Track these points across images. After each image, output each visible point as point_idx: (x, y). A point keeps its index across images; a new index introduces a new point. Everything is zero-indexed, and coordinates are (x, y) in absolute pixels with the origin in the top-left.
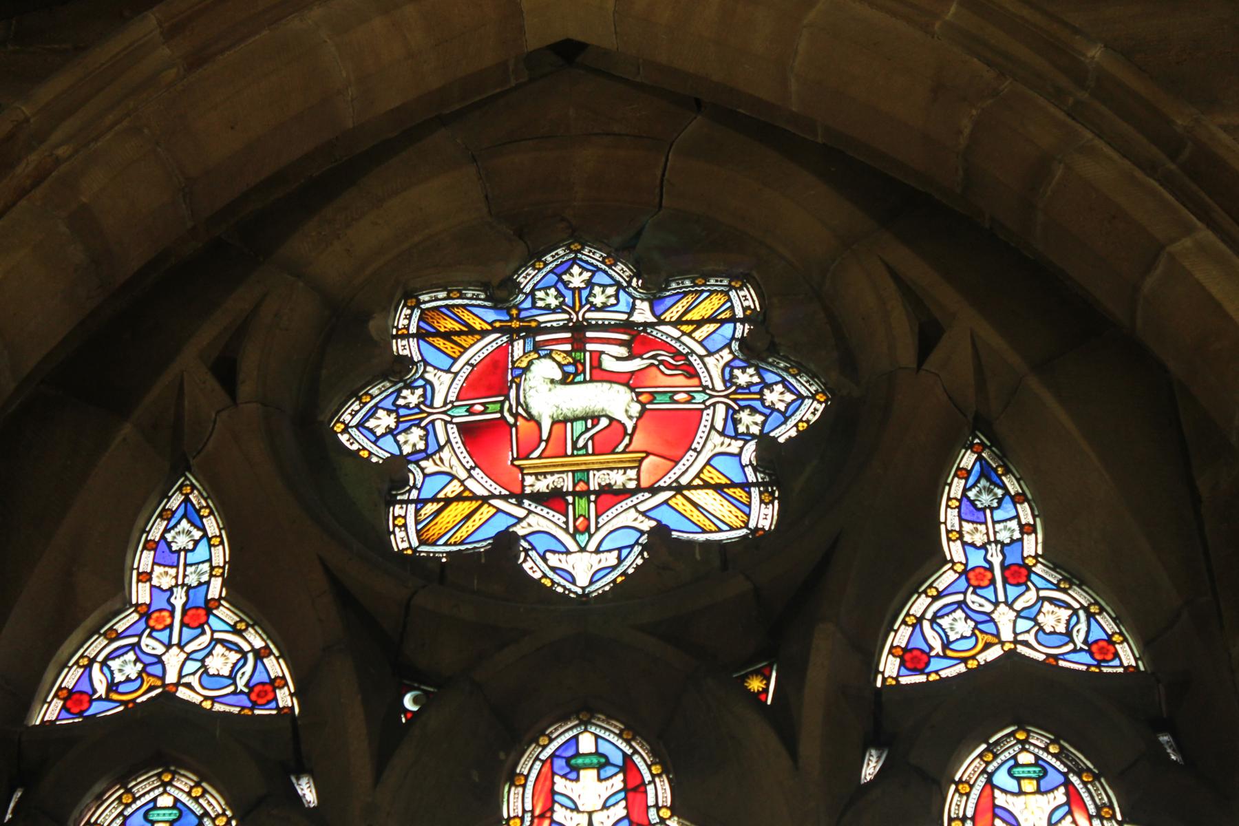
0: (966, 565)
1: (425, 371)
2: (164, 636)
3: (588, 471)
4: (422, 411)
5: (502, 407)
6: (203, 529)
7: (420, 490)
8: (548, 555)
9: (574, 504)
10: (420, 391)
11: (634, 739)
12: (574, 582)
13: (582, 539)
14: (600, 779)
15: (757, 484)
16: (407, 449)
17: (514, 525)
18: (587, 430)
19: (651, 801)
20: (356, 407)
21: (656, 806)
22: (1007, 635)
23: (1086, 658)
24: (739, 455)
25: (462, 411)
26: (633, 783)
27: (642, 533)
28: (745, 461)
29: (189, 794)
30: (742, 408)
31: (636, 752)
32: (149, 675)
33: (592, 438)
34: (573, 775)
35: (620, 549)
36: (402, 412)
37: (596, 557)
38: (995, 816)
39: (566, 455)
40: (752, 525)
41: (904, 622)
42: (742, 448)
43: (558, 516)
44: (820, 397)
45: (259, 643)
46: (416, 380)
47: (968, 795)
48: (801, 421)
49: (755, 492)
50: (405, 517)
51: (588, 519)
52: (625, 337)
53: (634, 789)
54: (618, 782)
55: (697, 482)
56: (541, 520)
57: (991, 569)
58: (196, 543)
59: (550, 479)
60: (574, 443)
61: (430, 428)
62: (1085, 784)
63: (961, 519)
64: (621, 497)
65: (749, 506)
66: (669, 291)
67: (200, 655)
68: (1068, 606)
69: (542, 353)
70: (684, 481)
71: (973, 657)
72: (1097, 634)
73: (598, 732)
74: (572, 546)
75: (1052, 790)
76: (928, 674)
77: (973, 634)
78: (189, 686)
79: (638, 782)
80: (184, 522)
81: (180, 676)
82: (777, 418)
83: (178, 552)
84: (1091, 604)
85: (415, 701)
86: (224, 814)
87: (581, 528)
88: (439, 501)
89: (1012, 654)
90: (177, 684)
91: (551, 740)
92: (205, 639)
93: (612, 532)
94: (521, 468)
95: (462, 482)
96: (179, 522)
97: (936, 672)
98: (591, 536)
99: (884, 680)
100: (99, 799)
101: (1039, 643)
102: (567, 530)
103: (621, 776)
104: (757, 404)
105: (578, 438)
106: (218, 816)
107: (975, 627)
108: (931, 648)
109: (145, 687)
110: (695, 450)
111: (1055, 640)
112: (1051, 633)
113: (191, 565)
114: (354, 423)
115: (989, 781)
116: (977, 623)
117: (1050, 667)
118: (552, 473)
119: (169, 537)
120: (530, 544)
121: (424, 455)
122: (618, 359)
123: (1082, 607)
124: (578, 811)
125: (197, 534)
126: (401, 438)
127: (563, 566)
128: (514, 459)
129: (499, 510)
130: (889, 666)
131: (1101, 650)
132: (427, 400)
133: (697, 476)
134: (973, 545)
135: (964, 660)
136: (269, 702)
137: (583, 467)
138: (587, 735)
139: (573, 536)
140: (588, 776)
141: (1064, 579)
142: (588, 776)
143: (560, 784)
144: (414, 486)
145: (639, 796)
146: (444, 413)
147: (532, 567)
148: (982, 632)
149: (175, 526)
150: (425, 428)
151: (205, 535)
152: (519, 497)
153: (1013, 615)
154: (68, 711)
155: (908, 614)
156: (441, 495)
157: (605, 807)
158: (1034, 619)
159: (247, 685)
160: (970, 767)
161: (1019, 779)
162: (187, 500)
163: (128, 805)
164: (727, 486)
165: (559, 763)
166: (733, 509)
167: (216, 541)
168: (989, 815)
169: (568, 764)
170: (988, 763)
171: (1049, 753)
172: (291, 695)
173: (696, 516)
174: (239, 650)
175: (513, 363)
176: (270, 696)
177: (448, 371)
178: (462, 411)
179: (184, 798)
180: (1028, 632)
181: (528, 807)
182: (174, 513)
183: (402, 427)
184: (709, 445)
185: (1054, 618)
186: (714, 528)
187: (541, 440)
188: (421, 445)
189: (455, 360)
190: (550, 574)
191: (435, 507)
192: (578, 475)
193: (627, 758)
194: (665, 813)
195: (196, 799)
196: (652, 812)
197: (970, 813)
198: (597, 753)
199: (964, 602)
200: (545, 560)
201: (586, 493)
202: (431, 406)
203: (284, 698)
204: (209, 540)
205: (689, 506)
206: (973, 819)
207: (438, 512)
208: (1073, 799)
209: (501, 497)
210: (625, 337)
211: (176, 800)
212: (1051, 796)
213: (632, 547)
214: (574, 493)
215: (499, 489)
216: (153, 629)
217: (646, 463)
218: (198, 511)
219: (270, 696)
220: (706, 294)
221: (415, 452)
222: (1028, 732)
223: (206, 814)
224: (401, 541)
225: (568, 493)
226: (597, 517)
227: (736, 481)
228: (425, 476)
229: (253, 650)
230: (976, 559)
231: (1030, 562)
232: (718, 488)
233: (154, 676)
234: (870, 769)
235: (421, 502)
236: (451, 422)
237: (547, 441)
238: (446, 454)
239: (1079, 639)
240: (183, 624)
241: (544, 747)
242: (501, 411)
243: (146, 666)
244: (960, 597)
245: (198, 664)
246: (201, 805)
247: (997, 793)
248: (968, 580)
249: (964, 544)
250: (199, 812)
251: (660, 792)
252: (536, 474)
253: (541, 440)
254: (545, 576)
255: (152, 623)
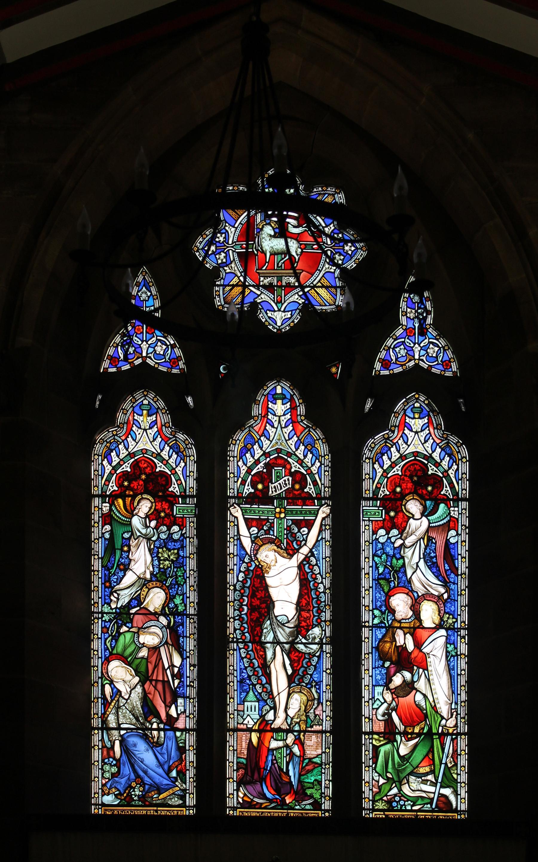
0: (406, 326)
1: (226, 226)
2: (140, 336)
3: (282, 276)
4: (225, 246)
5: (253, 247)
6: (150, 292)
7: (224, 279)
8: (268, 312)
9: (277, 290)
10: (224, 235)
11: (294, 389)
12: (276, 324)
13: (279, 305)
14: (283, 404)
15: (339, 287)
16: (220, 262)
17: (256, 298)
18: (282, 259)
19: (298, 413)
20: (201, 240)
21: (300, 415)
22: (417, 357)
23: (440, 367)
24: (334, 273)
25: (239, 247)
26: (294, 406)
27: (300, 304)
28: (336, 275)
29: (153, 400)
30: (336, 253)
31: (294, 394)
32: (137, 352)
33: (284, 263)
34: (274, 402)
35: (292, 311)
36: (218, 244)
37: (283, 314)
38: (405, 426)
39: (275, 270)
40: (337, 304)
41: (384, 349)
42: (335, 270)
43: (271, 295)
44: (364, 249)
45: (172, 342)
46: (222, 229)
47: (397, 417)
48: (356, 259)
49: (339, 290)
50: (219, 291)
51: (281, 297)
52: (296, 215)
53: (293, 408)
54: (288, 405)
55: (319, 284)
56: (265, 297)
57: (415, 329)
58: (149, 297)
59: (269, 279)
60: (278, 264)
61: (227, 253)
62: (434, 416)
63: (407, 307)
64: (293, 288)
65: (336, 295)
66: (313, 192)
67: (153, 346)
68: (438, 346)
69: (268, 221)
70: (315, 283)
71: (405, 365)
72: (446, 358)
73: (283, 385)
74: (276, 309)
75: (423, 418)
76: (390, 370)
77: (406, 355)
78: (150, 358)
79: (295, 405)
80: (144, 288)
81: (147, 354)
82: (348, 257)
83: (143, 301)
84: (445, 346)
85: (224, 369)
86: (164, 409)
87: (279, 300)
88: (230, 285)
89: (417, 366)
90: (146, 357)
91: (268, 387)
92: (154, 339)
93: (289, 303)
94: (259, 273)
95: (239, 277)
96: (142, 288)
97: (392, 370)
98: (282, 304)
99: (376, 371)
100: (125, 400)
101: (427, 361)
102: (274, 301)
103: (289, 403)
104: (341, 251)
105: (279, 262)
106: (163, 409)
107: (407, 353)
108: (392, 360)
109: (136, 357)
110: (319, 270)
111: (432, 359)
112: (431, 357)
113: (148, 307)
114: (200, 247)
115: (405, 413)
116: (408, 351)
117: (428, 371)
118: (270, 277)
119: (139, 294)
120: (262, 306)
121: (225, 264)
122: (294, 227)
123: (442, 347)
124: (276, 416)
125: (149, 294)
126: (217, 256)
127: (273, 317)
128: (257, 270)
129: (251, 291)
130: (378, 366)
131: (447, 365)
132: (226, 239)
133: (319, 281)
134: (410, 318)
135: (402, 365)
136: (176, 366)
137: (280, 275)
138: (279, 386)
139: (276, 304)
140: (279, 402)
141: (438, 335)
142: (279, 402)
143: (270, 405)
144: (222, 278)
145: (295, 411)
146: (232, 247)
147: (262, 317)
148: (409, 355)
149: (141, 290)
150: (225, 253)
151: (151, 294)
152: (257, 286)
153: (419, 348)
154: (112, 364)
155: (385, 346)
156: (231, 283)
157: (284, 415)
158: (426, 351)
159: (169, 359)
160: (399, 406)
161: (414, 413)
162: (144, 278)
163: (134, 403)
164: (329, 287)
165: (270, 396)
166: (331, 297)
167: (155, 297)
168: (403, 425)
169: (273, 397)
170: (405, 406)
171: (425, 404)
172: (183, 364)
173: (318, 299)
174: (166, 345)
175: (257, 225)
176: (177, 364)
177: (233, 227)
178: (239, 247)
179: (152, 402)
180: (424, 356)
181: (260, 412)
182: (140, 283)
183: (218, 251)
184: (324, 268)
185: (433, 351)
186: (324, 304)
187: (266, 262)
188: (224, 260)
189: (236, 221)
190: (268, 320)
191: (230, 288)
192: (278, 278)
193: (292, 396)
194: (303, 418)
195: (155, 402)
196: (299, 417)
197: (397, 425)
198: (282, 394)
199: (404, 342)
200: (267, 314)
201: (281, 286)
202: (228, 243)
203: (181, 364)
204: (153, 296)
205: (316, 294)
206: (398, 426)
207: (231, 290)
208: (430, 422)
209: (253, 286)
210: (296, 215)
211: (149, 402)
212: (423, 420)
213: (296, 310)
214: (277, 286)
215: (253, 283)
216: (137, 334)
217: (302, 274)
218: (149, 284)
219: (177, 364)
220: (327, 195)
221: (222, 263)
222: (419, 395)
223: (159, 408)
224: (218, 302)
225: (275, 286)
226: (285, 296)
227: (333, 285)
228: (226, 273)
229: (170, 344)
230: (410, 325)
231: (428, 327)
232: (327, 288)
233: (138, 353)
234: (368, 405)
235: (224, 286)
236: (235, 251)
237: (268, 262)
238: (233, 265)
239: (440, 360)
240: (147, 332)
241: (265, 390)
242: (252, 249)
243: (135, 348)
244: (403, 340)
245: (153, 349)
246: (157, 404)
247: (407, 418)
248: (407, 333)
249: (407, 317)
250: (157, 407)
251: (301, 410)
252: (264, 277)
253: (266, 262)
254: (266, 321)
255: (136, 331)
